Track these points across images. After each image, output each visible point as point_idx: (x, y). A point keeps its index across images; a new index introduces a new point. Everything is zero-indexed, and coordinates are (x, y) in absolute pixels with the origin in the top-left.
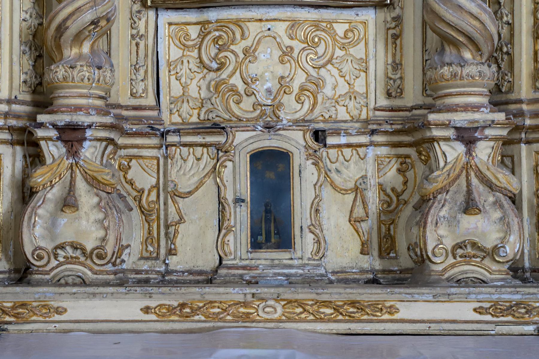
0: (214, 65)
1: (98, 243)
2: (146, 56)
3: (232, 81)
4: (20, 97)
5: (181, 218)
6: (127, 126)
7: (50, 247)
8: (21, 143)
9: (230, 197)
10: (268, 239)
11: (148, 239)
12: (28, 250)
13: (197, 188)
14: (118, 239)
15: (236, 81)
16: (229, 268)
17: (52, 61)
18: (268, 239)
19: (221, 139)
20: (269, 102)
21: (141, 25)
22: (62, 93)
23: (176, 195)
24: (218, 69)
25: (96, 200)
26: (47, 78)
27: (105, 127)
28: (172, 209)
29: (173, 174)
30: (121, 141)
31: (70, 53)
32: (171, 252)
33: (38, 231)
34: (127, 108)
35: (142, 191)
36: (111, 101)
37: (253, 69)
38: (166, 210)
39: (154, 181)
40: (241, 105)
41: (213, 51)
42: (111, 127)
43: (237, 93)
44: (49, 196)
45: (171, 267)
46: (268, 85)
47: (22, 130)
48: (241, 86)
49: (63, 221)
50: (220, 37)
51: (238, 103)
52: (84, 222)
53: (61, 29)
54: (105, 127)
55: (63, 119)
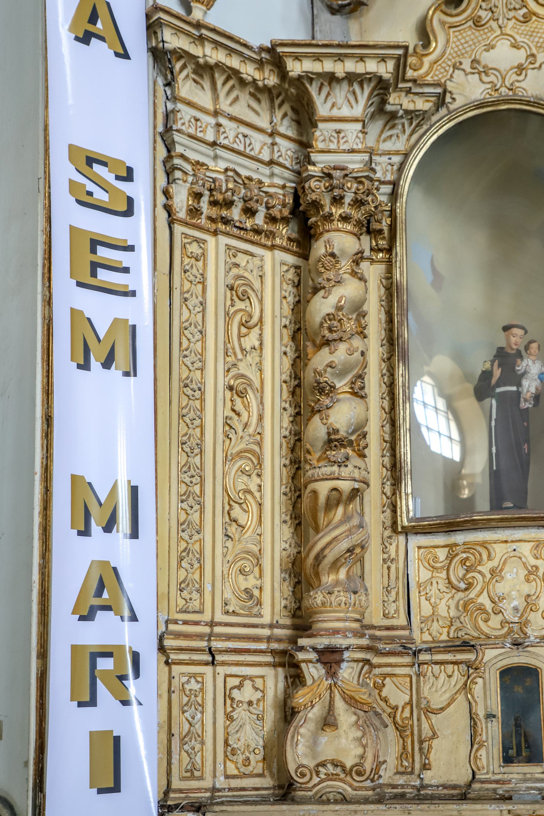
0: (463, 586)
1: (357, 761)
2: (397, 578)
3: (480, 600)
4: (281, 622)
5: (434, 734)
6: (381, 646)
7: (312, 764)
8: (282, 665)
9: (481, 713)
10: (519, 753)
11: (403, 754)
12: (292, 767)
13: (449, 705)
14: (376, 756)
15: (484, 600)
16: (483, 782)
17: (310, 586)
18: (519, 753)
19: (471, 656)
20: (516, 619)
21: (392, 549)
22: (321, 617)
23: (429, 711)
24: (466, 589)
25: (354, 718)
26: (306, 603)
27: (361, 648)
28: (425, 725)
29: (426, 691)
30: (376, 660)
31: (328, 579)
32: (425, 767)
33: (301, 749)
34: (380, 628)
35: (396, 708)
36: (366, 622)
37: (500, 588)
38: (419, 726)
39: (407, 698)
40: (490, 623)
41: (461, 572)
42: (368, 649)
43: (485, 611)
44: (310, 715)
45: (426, 782)
46: (515, 603)
47: (284, 653)
48: (489, 606)
49: (324, 739)
50: (467, 559)
51: (486, 621)
52: (343, 741)
53: (319, 558)
54: (361, 648)
55: (322, 642)
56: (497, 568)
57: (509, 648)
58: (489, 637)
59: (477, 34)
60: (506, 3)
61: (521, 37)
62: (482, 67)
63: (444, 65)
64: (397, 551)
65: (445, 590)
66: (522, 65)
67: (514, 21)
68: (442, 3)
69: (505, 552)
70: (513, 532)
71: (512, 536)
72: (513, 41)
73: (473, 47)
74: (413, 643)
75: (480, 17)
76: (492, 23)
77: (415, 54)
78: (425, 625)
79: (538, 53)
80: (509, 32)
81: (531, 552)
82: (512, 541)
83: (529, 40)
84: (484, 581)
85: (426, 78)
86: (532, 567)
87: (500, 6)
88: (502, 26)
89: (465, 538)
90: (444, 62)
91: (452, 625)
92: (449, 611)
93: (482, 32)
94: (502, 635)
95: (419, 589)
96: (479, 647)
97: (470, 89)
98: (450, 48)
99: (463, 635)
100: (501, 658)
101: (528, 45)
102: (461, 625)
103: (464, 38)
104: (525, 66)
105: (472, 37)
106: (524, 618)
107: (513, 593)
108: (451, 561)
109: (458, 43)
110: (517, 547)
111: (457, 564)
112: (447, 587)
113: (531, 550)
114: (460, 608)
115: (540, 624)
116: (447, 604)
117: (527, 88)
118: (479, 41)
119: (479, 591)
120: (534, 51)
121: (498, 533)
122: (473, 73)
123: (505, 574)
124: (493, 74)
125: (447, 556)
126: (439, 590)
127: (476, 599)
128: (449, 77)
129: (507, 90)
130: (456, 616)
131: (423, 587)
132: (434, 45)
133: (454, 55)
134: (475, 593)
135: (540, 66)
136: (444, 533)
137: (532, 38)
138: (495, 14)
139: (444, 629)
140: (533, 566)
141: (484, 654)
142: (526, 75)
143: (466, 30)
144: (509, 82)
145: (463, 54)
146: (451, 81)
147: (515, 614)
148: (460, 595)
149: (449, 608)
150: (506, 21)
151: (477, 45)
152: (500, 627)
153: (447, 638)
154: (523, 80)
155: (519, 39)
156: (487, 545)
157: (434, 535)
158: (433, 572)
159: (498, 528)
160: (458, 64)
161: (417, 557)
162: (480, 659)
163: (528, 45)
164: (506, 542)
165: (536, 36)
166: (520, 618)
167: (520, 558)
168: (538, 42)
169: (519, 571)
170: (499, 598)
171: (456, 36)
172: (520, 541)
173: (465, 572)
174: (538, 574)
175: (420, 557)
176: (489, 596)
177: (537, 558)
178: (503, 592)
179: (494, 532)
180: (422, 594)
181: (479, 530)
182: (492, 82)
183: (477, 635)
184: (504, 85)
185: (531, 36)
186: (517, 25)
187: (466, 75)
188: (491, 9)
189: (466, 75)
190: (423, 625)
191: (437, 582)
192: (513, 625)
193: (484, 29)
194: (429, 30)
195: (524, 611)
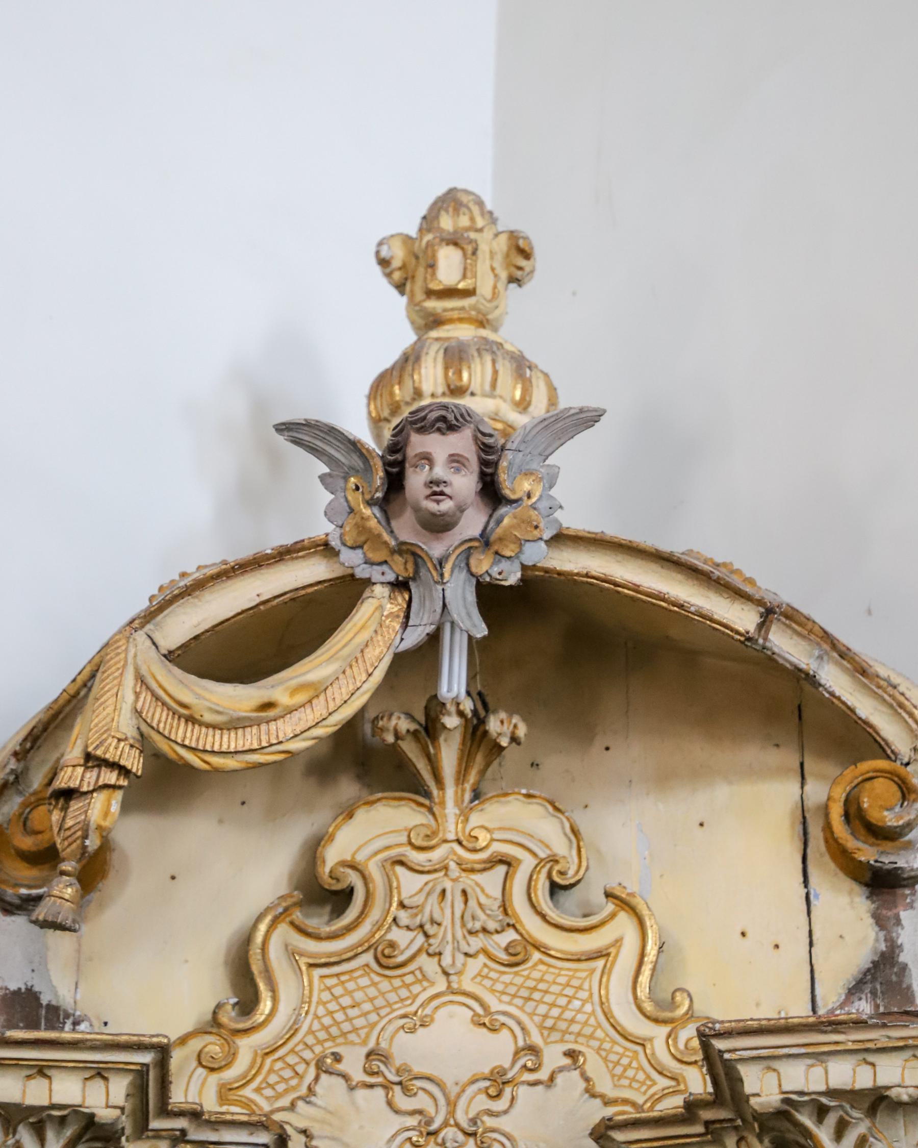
59: (385, 985)
60: (462, 917)
61: (500, 1001)
62: (393, 1071)
63: (292, 1060)
66: (502, 1072)
67: (482, 959)
68: (295, 904)
72: (480, 1010)
73: (373, 1017)
75: (392, 945)
76: (423, 959)
77: (214, 1030)
79: (546, 1043)
80: (468, 986)
83: (521, 1009)
85: (241, 1093)
87: (447, 922)
88: (451, 972)
90: (292, 1051)
93: (397, 983)
97: (361, 1127)
98: (310, 1017)
101: (519, 1023)
103: (349, 993)
104: (509, 1075)
105: (372, 992)
109: (333, 1006)
117: (515, 1134)
118: (389, 1005)
120: (536, 1039)
122: (371, 1086)
124: (424, 1090)
128: (303, 1091)
129: (461, 1137)
132: (266, 1005)
133: (322, 1035)
135: (552, 1078)
137: (530, 1006)
138: (432, 941)
142: (513, 1099)
143: (356, 974)
144: (467, 1113)
145: (344, 1034)
146: (308, 1103)
150: (460, 958)
151: (383, 1012)
154: (506, 1112)
155: (495, 1005)
160: (329, 1061)
163: (519, 1023)
165: (541, 1001)
168: (546, 1016)
171: (329, 989)
182: (420, 1112)
184: (452, 1122)
185: (529, 999)
186: (491, 970)
187: (352, 1089)
188: (421, 926)
189: (352, 1089)
193: (404, 975)
194: (256, 968)
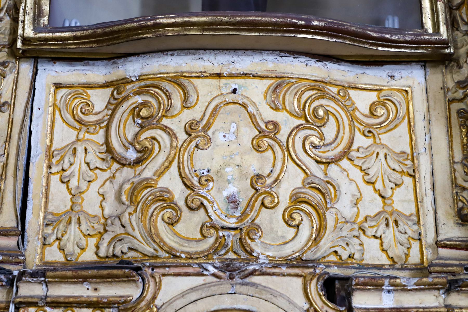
0: (132, 155)
3: (163, 183)
20: (232, 222)
24: (138, 162)
40: (179, 227)
46: (231, 190)
50: (145, 104)
51: (172, 223)
56: (198, 123)
57: (214, 275)
58: (175, 256)
64: (15, 90)
65: (99, 164)
69: (216, 94)
70: (232, 59)
71: (231, 67)
74: (18, 263)
78: (53, 230)
81: (265, 97)
82: (231, 76)
84: (172, 146)
86: (267, 124)
89: (143, 68)
91: (106, 231)
92: (104, 204)
94: (203, 252)
95: (49, 161)
96: (150, 271)
99: (125, 250)
100: (194, 296)
102: (122, 231)
106: (248, 220)
107: (228, 169)
108: (114, 111)
110: (240, 86)
111: (126, 115)
112: (103, 159)
113: (266, 93)
114: (124, 198)
115: (280, 234)
116: (101, 191)
119: (163, 164)
121: (205, 58)
123: (213, 133)
125: (109, 103)
126: (88, 164)
127: (156, 181)
130: (115, 214)
131: (59, 157)
134: (155, 169)
136: (106, 62)
139: (89, 239)
140: (269, 122)
141: (158, 287)
147: (231, 211)
148: (127, 172)
149: (104, 199)
152: (199, 236)
153: (95, 258)
156: (182, 80)
157: (88, 64)
158: (80, 130)
159: (205, 49)
161: (51, 103)
162: (149, 296)
164: (219, 76)
166: (240, 219)
167: (244, 106)
169: (242, 129)
170: (200, 179)
172: (245, 75)
173: (138, 129)
174: (278, 136)
175: (57, 103)
176: (180, 175)
177: (277, 109)
178: (209, 167)
179: (197, 57)
180: (54, 170)
181: (170, 53)
183: (152, 250)
190: (49, 230)
191: (86, 150)
192: (226, 233)
195: (248, 206)
